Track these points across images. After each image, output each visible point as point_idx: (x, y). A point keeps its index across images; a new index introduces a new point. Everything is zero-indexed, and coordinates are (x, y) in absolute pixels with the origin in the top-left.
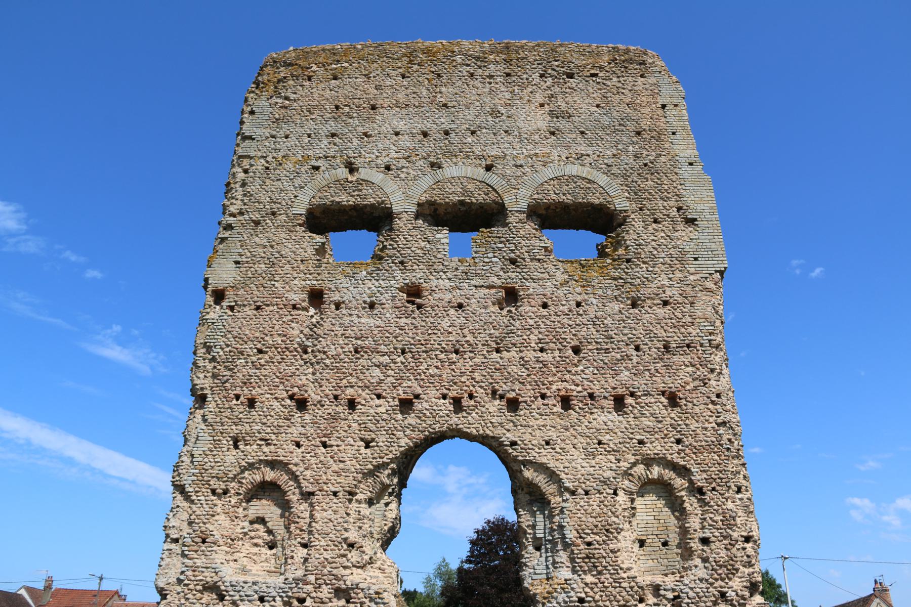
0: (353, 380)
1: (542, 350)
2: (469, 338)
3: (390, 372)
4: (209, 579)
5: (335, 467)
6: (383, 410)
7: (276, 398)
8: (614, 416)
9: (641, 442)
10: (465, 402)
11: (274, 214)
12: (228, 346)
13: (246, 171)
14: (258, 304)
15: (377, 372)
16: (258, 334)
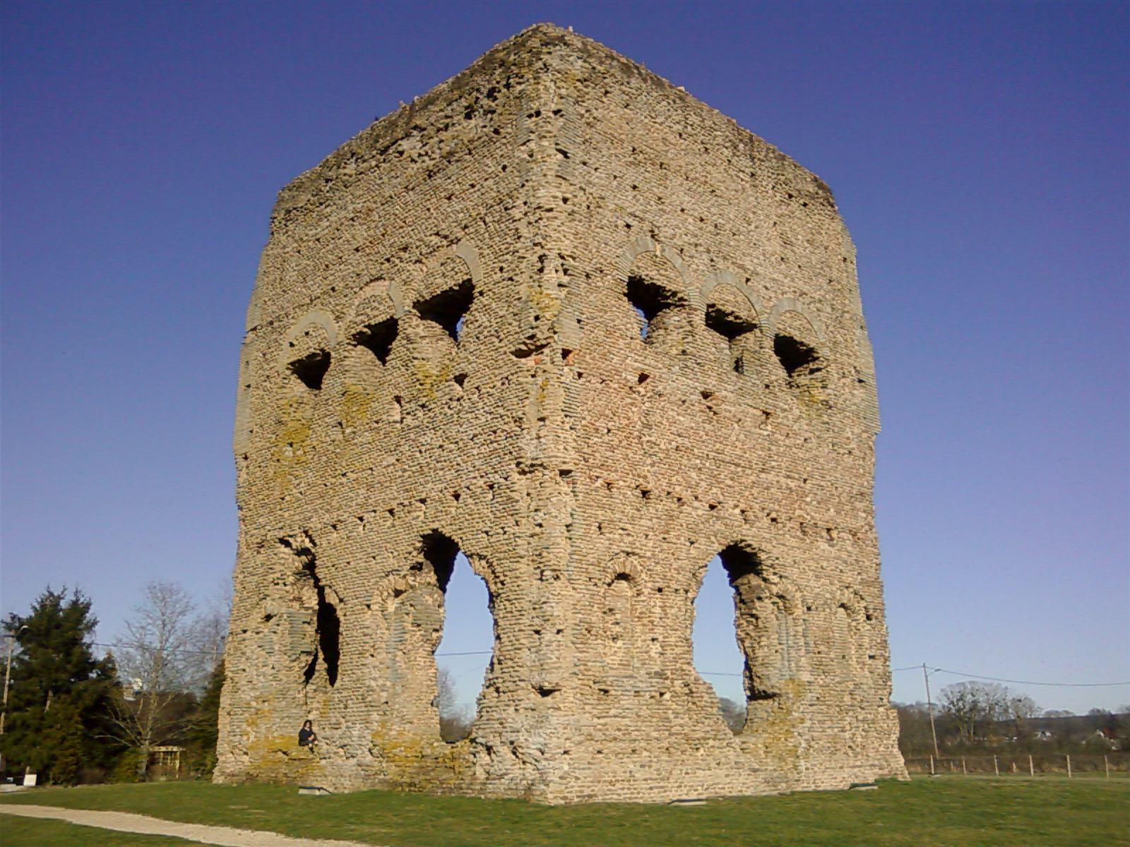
0: (680, 479)
1: (788, 477)
2: (747, 455)
3: (703, 477)
4: (597, 674)
5: (675, 566)
6: (700, 512)
7: (629, 487)
8: (824, 545)
9: (841, 571)
10: (750, 514)
11: (601, 271)
12: (584, 419)
13: (565, 200)
14: (604, 378)
15: (694, 475)
16: (607, 412)
